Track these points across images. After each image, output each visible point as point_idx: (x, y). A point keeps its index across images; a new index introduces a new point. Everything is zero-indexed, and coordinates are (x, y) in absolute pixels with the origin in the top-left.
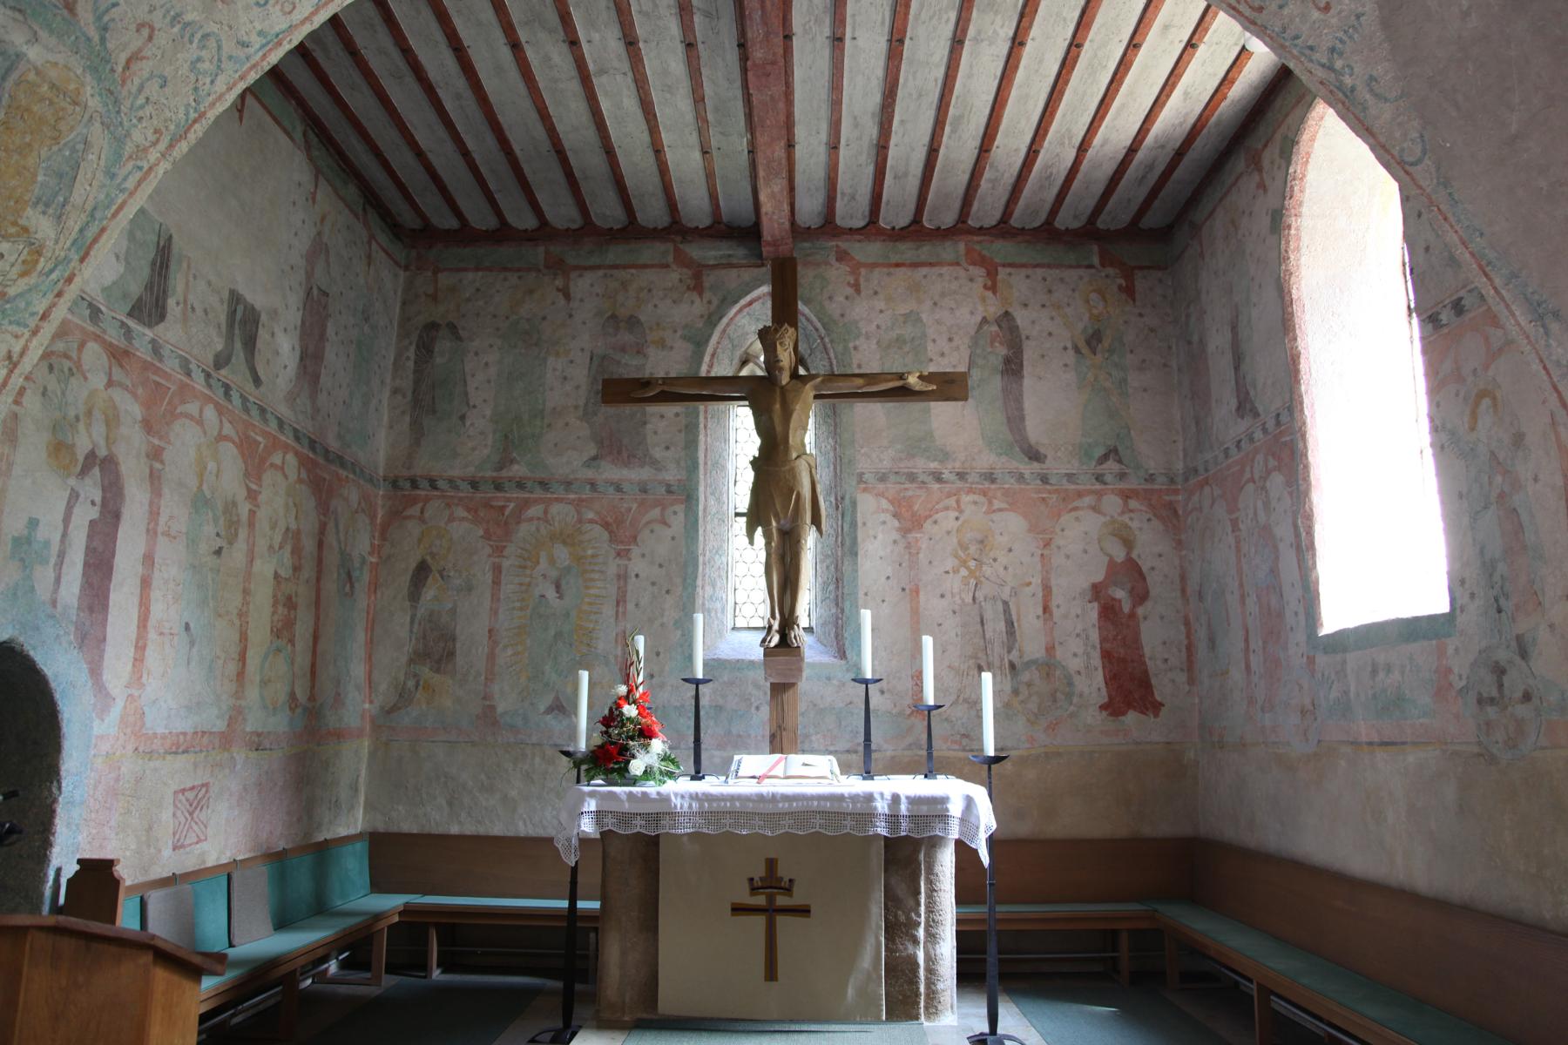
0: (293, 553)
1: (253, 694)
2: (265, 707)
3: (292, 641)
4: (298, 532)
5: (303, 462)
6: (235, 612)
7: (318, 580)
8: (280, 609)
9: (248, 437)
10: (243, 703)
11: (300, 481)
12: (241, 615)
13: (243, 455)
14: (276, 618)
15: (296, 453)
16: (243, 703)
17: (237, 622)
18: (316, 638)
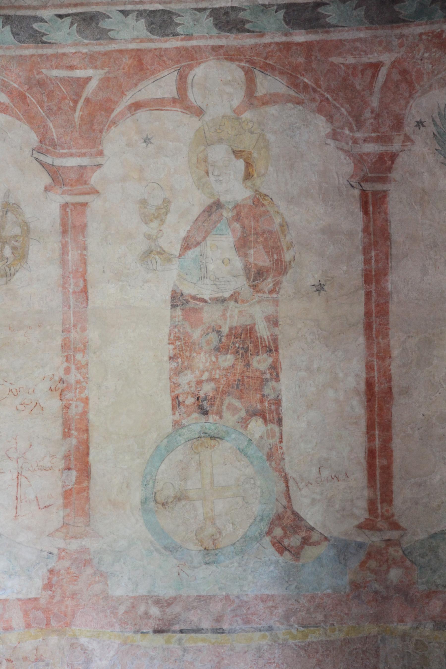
0: (242, 245)
1: (120, 525)
2: (172, 549)
3: (271, 414)
4: (259, 200)
5: (254, 63)
6: (44, 386)
7: (374, 277)
8: (202, 360)
9: (41, 84)
10: (86, 542)
11: (251, 97)
12: (61, 389)
13: (31, 119)
14: (187, 379)
15: (230, 55)
16: (92, 544)
17: (54, 404)
18: (378, 398)
